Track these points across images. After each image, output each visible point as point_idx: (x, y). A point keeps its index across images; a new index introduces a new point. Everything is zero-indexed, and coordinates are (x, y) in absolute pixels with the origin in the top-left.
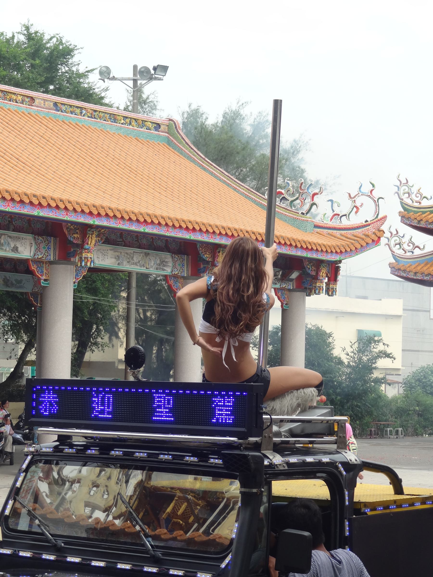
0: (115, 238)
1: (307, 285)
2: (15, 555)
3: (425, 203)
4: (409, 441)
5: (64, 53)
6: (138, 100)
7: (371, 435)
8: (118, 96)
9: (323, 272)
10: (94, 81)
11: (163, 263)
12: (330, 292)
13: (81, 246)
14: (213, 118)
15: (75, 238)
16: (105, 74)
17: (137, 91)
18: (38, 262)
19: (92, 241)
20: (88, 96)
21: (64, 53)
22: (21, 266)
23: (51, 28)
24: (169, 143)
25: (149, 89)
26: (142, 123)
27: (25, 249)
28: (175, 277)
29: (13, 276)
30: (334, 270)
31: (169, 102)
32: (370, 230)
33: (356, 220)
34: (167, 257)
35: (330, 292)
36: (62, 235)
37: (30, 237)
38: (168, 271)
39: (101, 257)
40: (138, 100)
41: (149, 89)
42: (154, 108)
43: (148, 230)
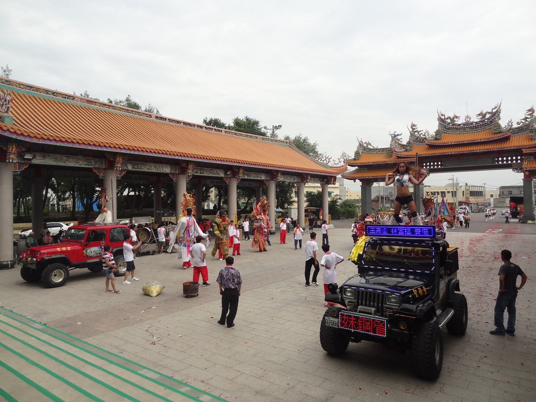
0: (284, 173)
1: (328, 182)
2: (369, 268)
3: (350, 158)
4: (347, 220)
5: (257, 123)
6: (273, 135)
7: (336, 219)
8: (269, 133)
9: (333, 179)
10: (263, 130)
11: (294, 179)
12: (334, 184)
13: (277, 176)
14: (292, 138)
15: (275, 174)
16: (265, 128)
17: (273, 132)
18: (265, 180)
19: (279, 175)
20: (264, 134)
21: (257, 123)
22: (261, 182)
23: (253, 117)
24: (290, 147)
25: (277, 132)
26: (276, 141)
27: (263, 178)
28: (297, 182)
29: (250, 183)
30: (335, 178)
31: (281, 135)
32: (344, 167)
33: (339, 165)
34: (295, 177)
35: (334, 184)
36: (272, 173)
37: (264, 174)
38: (296, 181)
39: (281, 179)
40: (273, 135)
41: (277, 132)
42: (277, 136)
43: (293, 171)
